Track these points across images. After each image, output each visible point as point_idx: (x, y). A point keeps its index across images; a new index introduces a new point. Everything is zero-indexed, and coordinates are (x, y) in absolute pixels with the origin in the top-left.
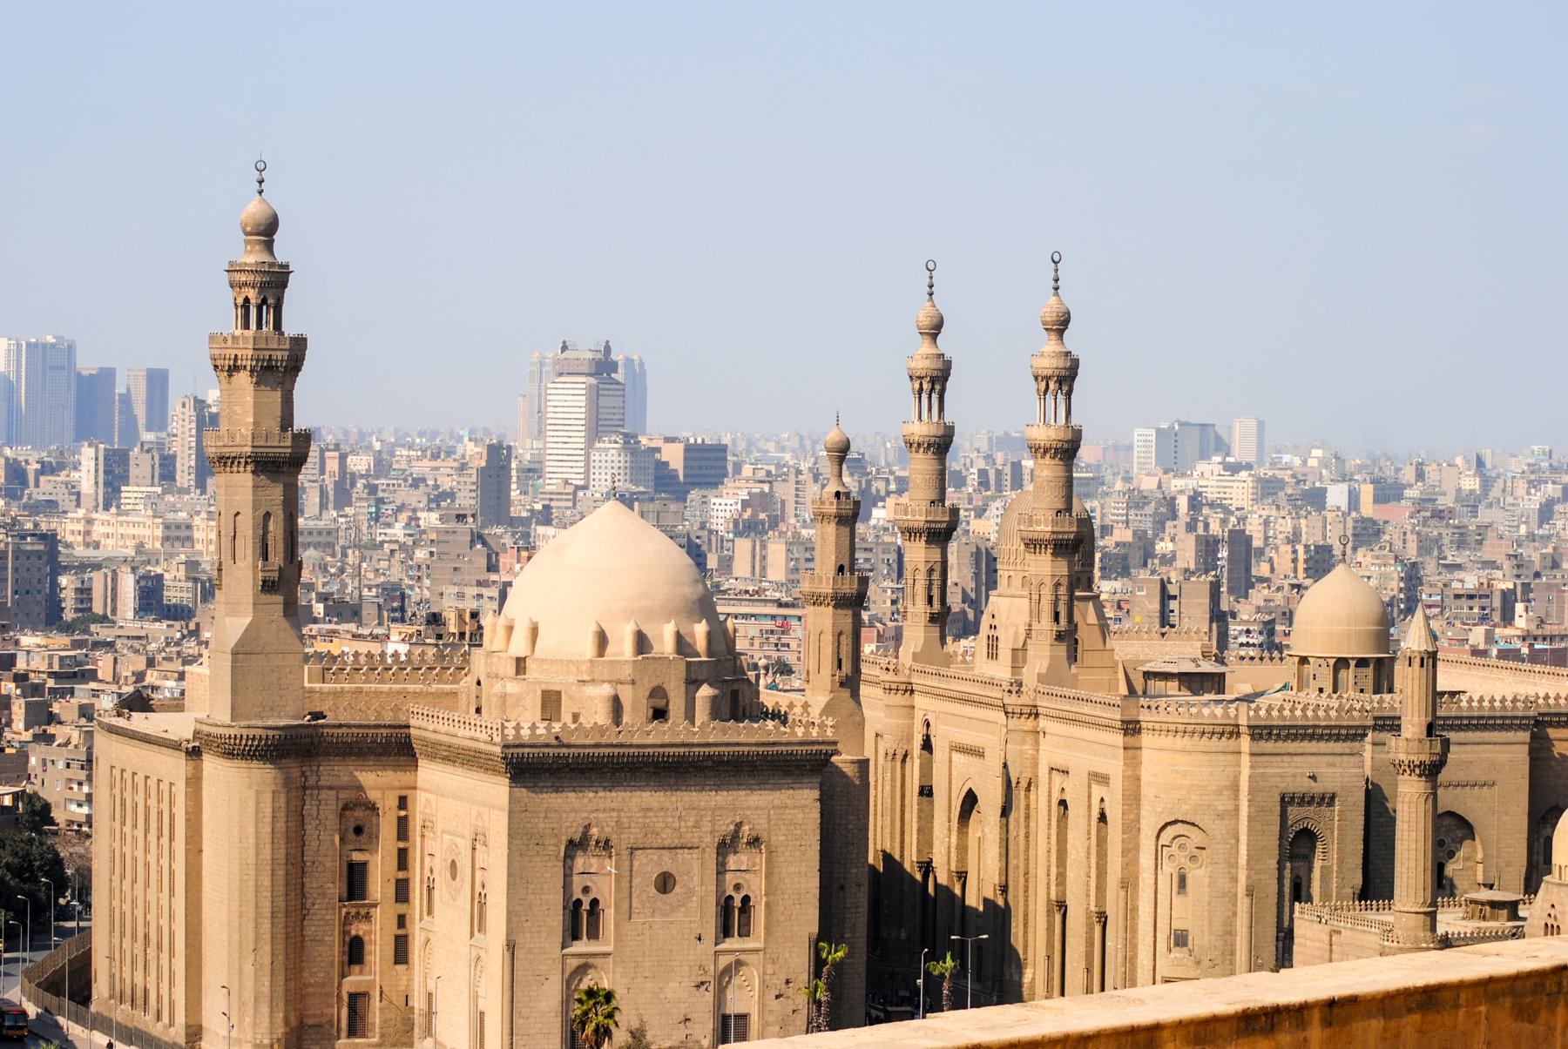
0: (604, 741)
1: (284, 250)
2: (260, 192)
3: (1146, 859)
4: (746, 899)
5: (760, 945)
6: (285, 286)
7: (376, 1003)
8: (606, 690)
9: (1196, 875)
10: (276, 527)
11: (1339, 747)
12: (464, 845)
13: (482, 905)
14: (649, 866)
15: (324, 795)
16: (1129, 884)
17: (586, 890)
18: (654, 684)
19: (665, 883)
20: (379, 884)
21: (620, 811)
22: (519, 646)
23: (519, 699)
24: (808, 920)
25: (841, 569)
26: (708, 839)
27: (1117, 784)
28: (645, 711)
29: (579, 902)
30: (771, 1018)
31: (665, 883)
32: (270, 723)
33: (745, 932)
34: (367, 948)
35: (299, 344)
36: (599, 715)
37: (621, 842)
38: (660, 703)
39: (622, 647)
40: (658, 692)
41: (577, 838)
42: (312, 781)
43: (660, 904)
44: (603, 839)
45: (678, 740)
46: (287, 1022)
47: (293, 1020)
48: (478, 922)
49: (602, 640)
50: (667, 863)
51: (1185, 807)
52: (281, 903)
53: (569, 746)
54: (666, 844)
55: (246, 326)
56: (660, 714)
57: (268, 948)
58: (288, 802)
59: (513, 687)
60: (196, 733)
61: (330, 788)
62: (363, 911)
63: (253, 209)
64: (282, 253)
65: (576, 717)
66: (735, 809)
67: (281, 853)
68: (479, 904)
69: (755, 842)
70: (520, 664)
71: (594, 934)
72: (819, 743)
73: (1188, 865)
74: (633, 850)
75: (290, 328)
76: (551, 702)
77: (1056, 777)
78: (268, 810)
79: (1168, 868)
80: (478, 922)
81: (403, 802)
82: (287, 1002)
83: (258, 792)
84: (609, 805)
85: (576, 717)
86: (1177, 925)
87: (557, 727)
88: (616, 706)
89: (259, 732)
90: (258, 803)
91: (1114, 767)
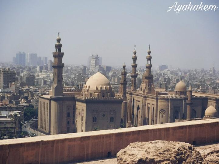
1: (61, 43)
3: (158, 114)
6: (61, 47)
8: (97, 93)
9: (164, 115)
12: (81, 111)
13: (83, 118)
16: (156, 116)
17: (95, 116)
19: (104, 115)
20: (71, 115)
22: (87, 88)
23: (87, 94)
27: (155, 105)
29: (94, 117)
31: (104, 115)
35: (63, 53)
39: (99, 89)
48: (82, 120)
49: (97, 88)
50: (104, 114)
59: (87, 93)
60: (51, 98)
64: (61, 43)
68: (82, 117)
69: (114, 111)
70: (88, 91)
75: (62, 52)
77: (148, 105)
79: (161, 115)
80: (82, 120)
81: (74, 106)
85: (94, 96)
86: (162, 121)
91: (155, 103)
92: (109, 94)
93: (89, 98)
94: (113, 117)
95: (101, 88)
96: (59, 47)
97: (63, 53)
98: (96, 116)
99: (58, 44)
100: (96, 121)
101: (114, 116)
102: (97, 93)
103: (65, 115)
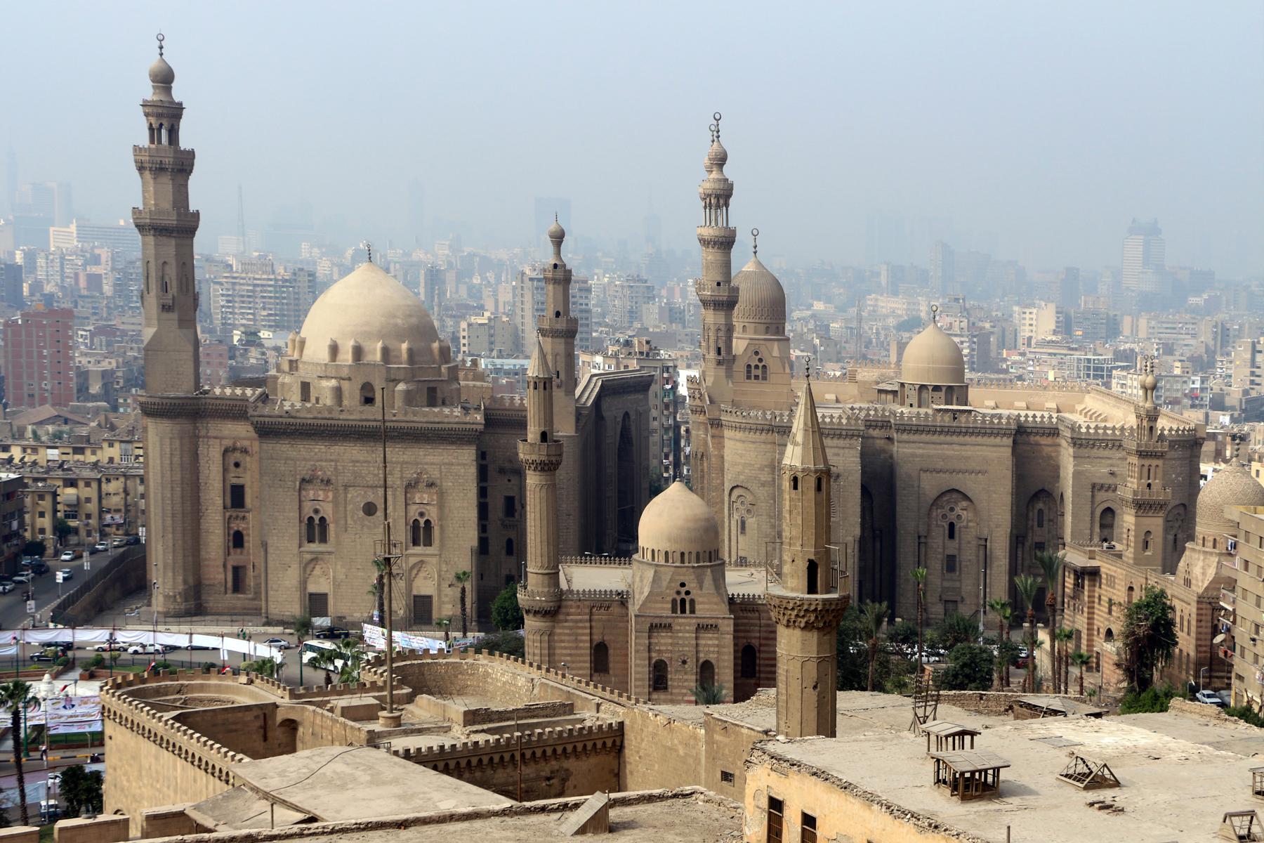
4: (428, 522)
10: (172, 272)
14: (357, 498)
15: (211, 442)
17: (316, 511)
21: (336, 461)
24: (469, 536)
29: (311, 519)
30: (446, 599)
33: (428, 543)
34: (246, 538)
41: (307, 478)
42: (203, 433)
51: (742, 477)
57: (170, 536)
58: (182, 444)
62: (241, 515)
65: (317, 399)
66: (417, 464)
67: (178, 477)
69: (431, 485)
71: (324, 539)
73: (746, 515)
79: (736, 516)
82: (185, 570)
86: (741, 554)
87: (308, 405)
88: (338, 392)
89: (157, 400)
90: (162, 445)
94: (428, 522)
98: (327, 511)
100: (324, 539)
101: (432, 514)
103: (214, 498)
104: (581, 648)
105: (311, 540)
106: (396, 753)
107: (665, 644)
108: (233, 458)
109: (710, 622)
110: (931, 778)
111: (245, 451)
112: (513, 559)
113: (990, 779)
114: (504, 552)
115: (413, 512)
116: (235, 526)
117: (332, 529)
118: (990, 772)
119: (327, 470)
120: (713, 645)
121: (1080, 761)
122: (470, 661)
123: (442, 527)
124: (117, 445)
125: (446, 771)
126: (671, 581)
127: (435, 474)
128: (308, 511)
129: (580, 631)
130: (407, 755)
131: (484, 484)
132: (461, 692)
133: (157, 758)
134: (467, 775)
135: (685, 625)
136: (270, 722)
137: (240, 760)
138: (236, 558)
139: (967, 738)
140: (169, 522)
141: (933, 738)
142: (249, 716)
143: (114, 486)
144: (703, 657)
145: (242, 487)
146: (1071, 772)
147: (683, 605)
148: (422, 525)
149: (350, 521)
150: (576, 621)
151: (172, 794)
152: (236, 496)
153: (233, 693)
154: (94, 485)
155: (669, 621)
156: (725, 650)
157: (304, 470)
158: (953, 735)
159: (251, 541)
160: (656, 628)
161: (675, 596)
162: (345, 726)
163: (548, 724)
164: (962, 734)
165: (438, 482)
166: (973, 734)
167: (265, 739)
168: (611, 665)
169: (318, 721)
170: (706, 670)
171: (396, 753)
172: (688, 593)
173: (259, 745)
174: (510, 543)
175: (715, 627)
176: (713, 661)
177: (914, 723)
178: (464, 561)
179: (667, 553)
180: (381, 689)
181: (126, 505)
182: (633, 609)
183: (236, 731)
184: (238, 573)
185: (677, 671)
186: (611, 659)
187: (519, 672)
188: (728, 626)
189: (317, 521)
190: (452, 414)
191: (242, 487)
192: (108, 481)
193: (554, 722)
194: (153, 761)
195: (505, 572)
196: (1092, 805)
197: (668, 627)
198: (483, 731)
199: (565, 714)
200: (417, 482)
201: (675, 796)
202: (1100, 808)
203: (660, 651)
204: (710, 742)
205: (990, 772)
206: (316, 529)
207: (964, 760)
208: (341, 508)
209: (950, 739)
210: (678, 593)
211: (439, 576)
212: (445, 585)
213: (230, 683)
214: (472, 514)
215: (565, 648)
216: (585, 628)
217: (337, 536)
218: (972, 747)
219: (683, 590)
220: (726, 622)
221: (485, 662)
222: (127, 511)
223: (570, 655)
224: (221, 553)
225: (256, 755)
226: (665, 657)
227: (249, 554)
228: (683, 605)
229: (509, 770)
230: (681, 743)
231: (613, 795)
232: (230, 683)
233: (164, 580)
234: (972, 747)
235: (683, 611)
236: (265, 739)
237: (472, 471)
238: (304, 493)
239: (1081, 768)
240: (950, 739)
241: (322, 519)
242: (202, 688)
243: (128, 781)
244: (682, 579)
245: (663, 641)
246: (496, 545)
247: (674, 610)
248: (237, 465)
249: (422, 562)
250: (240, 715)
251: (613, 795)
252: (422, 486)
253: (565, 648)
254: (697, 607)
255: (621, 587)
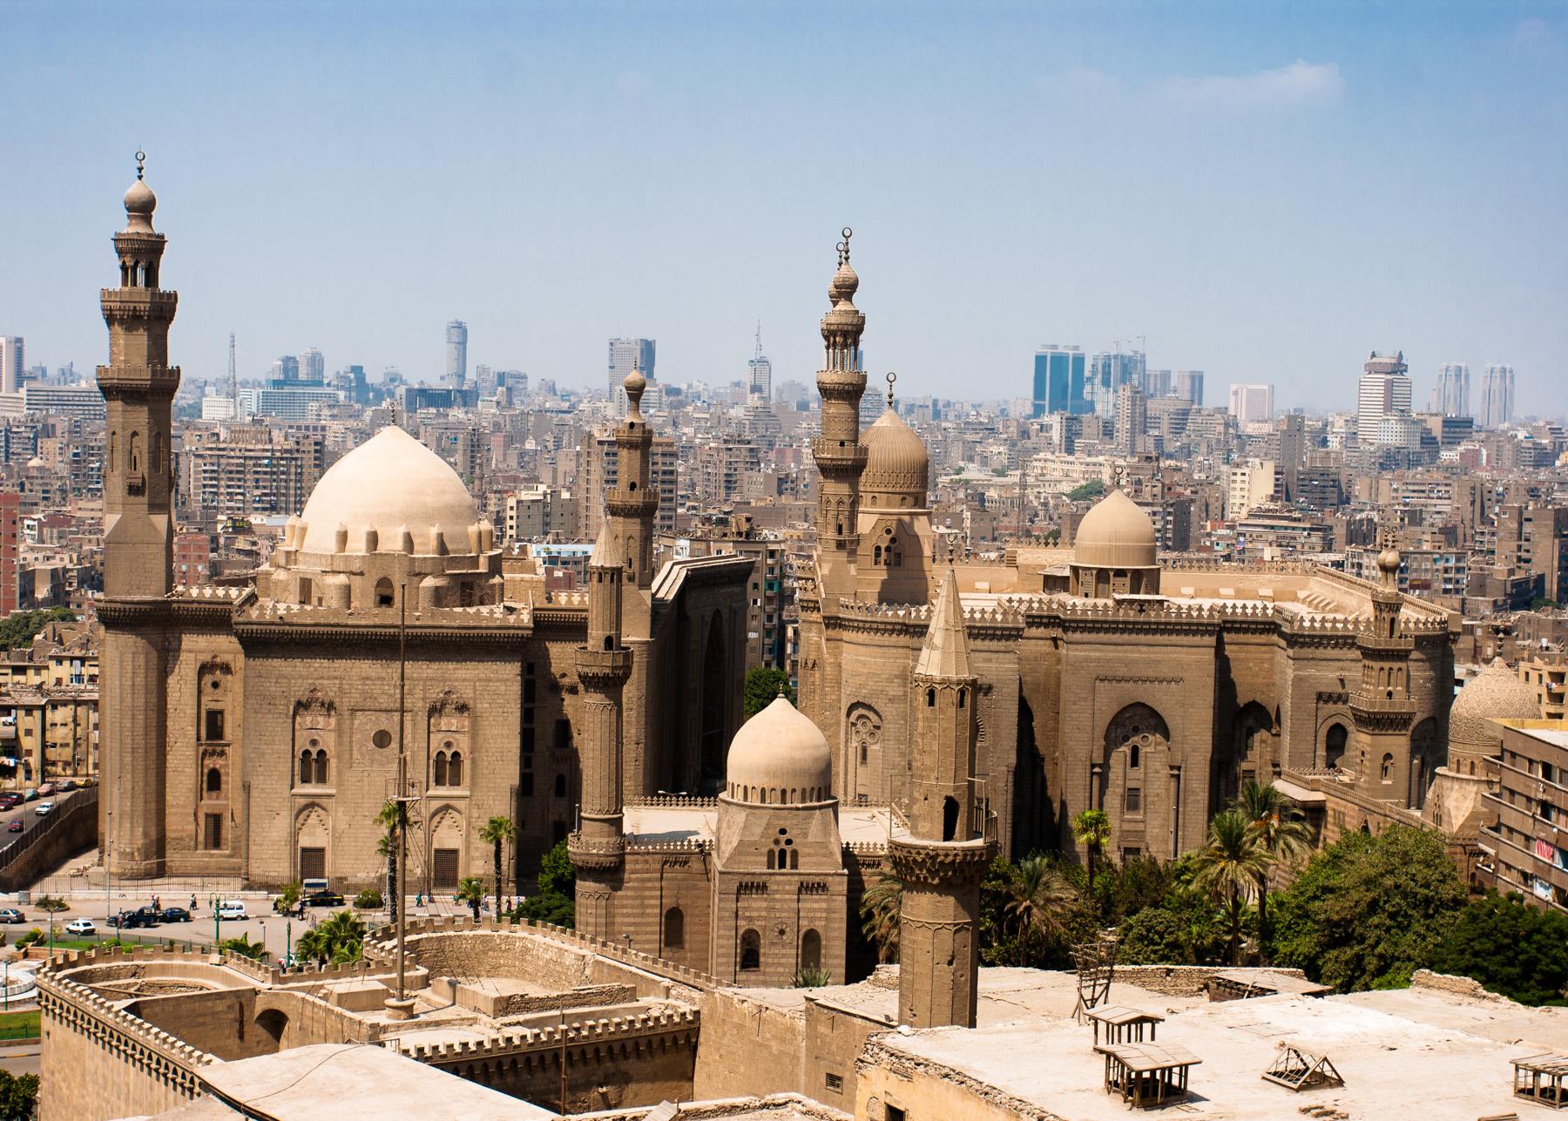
0: (322, 621)
1: (160, 223)
2: (140, 177)
4: (456, 755)
5: (467, 793)
6: (160, 251)
7: (227, 823)
8: (342, 579)
9: (874, 748)
11: (994, 645)
14: (367, 725)
17: (314, 742)
18: (381, 576)
21: (342, 679)
24: (509, 773)
25: (633, 486)
26: (420, 704)
28: (371, 597)
32: (129, 598)
33: (456, 782)
34: (224, 778)
35: (172, 298)
36: (333, 601)
37: (344, 704)
38: (386, 592)
39: (358, 546)
40: (384, 583)
41: (304, 700)
43: (377, 757)
44: (327, 701)
45: (389, 622)
46: (146, 834)
47: (153, 833)
49: (343, 537)
52: (140, 741)
53: (291, 625)
54: (383, 706)
55: (125, 283)
56: (386, 600)
58: (147, 662)
61: (190, 651)
62: (219, 749)
63: (136, 190)
66: (445, 680)
67: (141, 702)
69: (462, 708)
71: (322, 779)
72: (513, 628)
74: (353, 711)
75: (164, 285)
76: (306, 586)
78: (129, 668)
83: (122, 654)
84: (332, 673)
85: (320, 600)
86: (861, 790)
90: (122, 661)
92: (429, 582)
93: (288, 608)
94: (456, 755)
95: (373, 539)
96: (143, 255)
97: (172, 298)
98: (328, 742)
99: (131, 230)
100: (322, 779)
101: (463, 745)
102: (342, 579)
104: (649, 915)
105: (306, 780)
106: (406, 1052)
107: (757, 909)
108: (208, 679)
109: (817, 879)
110: (1102, 1083)
111: (226, 669)
112: (564, 802)
113: (1175, 1081)
114: (552, 791)
115: (437, 743)
116: (210, 763)
117: (333, 764)
118: (1176, 1070)
119: (329, 691)
120: (820, 910)
121: (1293, 1054)
122: (504, 932)
123: (474, 761)
124: (67, 663)
125: (471, 1076)
126: (768, 826)
127: (466, 693)
128: (302, 744)
129: (647, 893)
130: (421, 1055)
131: (530, 705)
132: (493, 972)
133: (104, 1059)
134: (496, 1081)
135: (784, 883)
136: (246, 1014)
137: (209, 1062)
138: (210, 803)
139: (1147, 1027)
140: (128, 759)
141: (1102, 1026)
142: (221, 1006)
143: (62, 714)
144: (805, 925)
145: (221, 712)
146: (1281, 1068)
147: (782, 857)
148: (449, 758)
149: (356, 755)
150: (643, 880)
151: (123, 1106)
152: (213, 725)
153: (201, 976)
154: (37, 714)
155: (764, 878)
156: (836, 916)
157: (300, 691)
158: (1129, 1023)
159: (231, 782)
160: (750, 887)
161: (772, 846)
162: (341, 1017)
163: (603, 1014)
164: (1141, 1020)
165: (471, 704)
166: (1153, 1021)
167: (241, 1037)
168: (687, 937)
169: (308, 1011)
170: (811, 943)
171: (406, 1052)
172: (789, 842)
173: (233, 1042)
174: (560, 780)
175: (822, 887)
176: (820, 931)
177: (1078, 1007)
178: (502, 806)
179: (763, 790)
180: (390, 971)
181: (76, 739)
182: (717, 863)
183: (204, 1024)
184: (215, 821)
185: (772, 944)
186: (687, 928)
187: (566, 946)
188: (840, 886)
189: (314, 756)
190: (489, 614)
191: (221, 712)
192: (55, 707)
193: (610, 1012)
194: (100, 1063)
195: (552, 818)
196: (1306, 1111)
197: (762, 888)
198: (518, 1023)
199: (624, 1000)
200: (443, 705)
201: (765, 1106)
202: (1317, 1116)
203: (750, 919)
204: (812, 1035)
205: (1176, 1070)
206: (313, 765)
207: (1142, 1057)
208: (346, 739)
209: (1124, 1029)
210: (777, 842)
211: (469, 824)
212: (476, 836)
213: (198, 963)
214: (514, 744)
215: (628, 915)
216: (653, 889)
217: (339, 773)
218: (1153, 1038)
219: (783, 838)
220: (837, 879)
221: (525, 934)
222: (76, 745)
223: (634, 924)
224: (192, 797)
225: (228, 1056)
226: (757, 925)
227: (226, 798)
228: (782, 857)
229: (551, 1074)
230: (775, 1037)
231: (684, 1106)
232: (198, 963)
233: (120, 831)
234: (1153, 1038)
235: (782, 866)
236: (241, 1037)
237: (516, 688)
238: (298, 719)
239: (1294, 1064)
240: (1124, 1029)
241: (322, 753)
242: (163, 970)
243: (68, 1088)
244: (783, 824)
245: (755, 905)
246: (544, 783)
247: (771, 866)
248: (215, 685)
249: (447, 807)
250: (210, 1004)
251: (684, 1106)
252: (449, 708)
253: (628, 915)
254: (801, 860)
255: (704, 836)
